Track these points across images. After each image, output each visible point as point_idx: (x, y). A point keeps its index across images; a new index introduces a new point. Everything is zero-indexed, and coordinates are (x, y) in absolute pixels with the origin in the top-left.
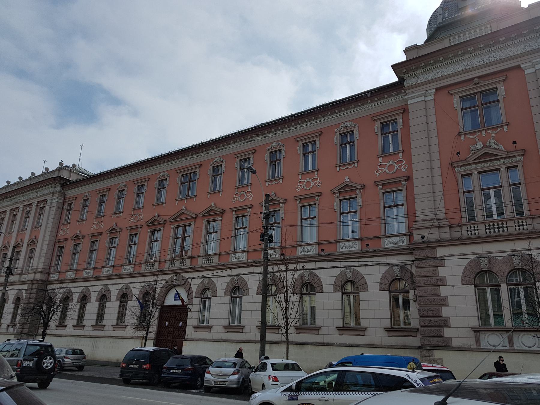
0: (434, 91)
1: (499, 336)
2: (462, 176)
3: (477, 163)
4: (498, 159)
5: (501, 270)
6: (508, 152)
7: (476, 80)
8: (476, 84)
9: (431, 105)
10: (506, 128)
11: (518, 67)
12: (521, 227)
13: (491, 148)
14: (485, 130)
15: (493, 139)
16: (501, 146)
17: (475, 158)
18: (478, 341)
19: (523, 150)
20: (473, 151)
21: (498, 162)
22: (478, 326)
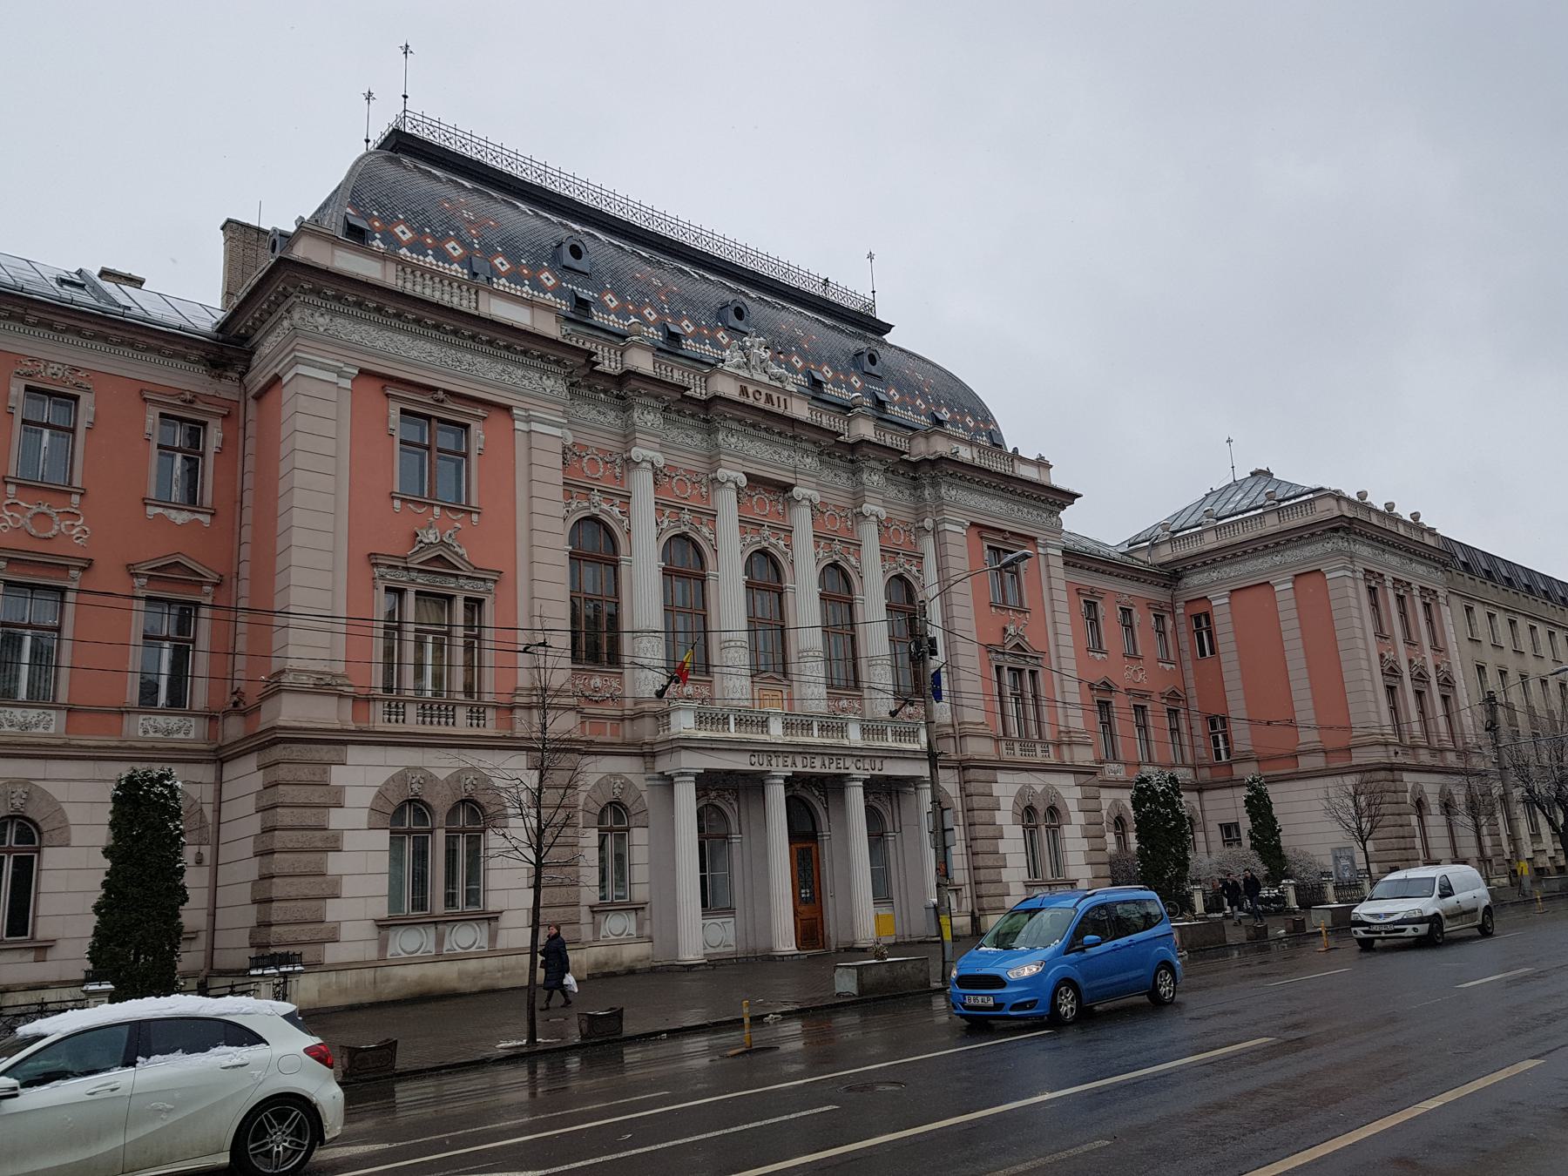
0: (356, 372)
3: (420, 571)
4: (456, 576)
5: (441, 803)
7: (441, 395)
8: (437, 401)
14: (442, 507)
17: (425, 558)
20: (422, 545)
21: (453, 580)
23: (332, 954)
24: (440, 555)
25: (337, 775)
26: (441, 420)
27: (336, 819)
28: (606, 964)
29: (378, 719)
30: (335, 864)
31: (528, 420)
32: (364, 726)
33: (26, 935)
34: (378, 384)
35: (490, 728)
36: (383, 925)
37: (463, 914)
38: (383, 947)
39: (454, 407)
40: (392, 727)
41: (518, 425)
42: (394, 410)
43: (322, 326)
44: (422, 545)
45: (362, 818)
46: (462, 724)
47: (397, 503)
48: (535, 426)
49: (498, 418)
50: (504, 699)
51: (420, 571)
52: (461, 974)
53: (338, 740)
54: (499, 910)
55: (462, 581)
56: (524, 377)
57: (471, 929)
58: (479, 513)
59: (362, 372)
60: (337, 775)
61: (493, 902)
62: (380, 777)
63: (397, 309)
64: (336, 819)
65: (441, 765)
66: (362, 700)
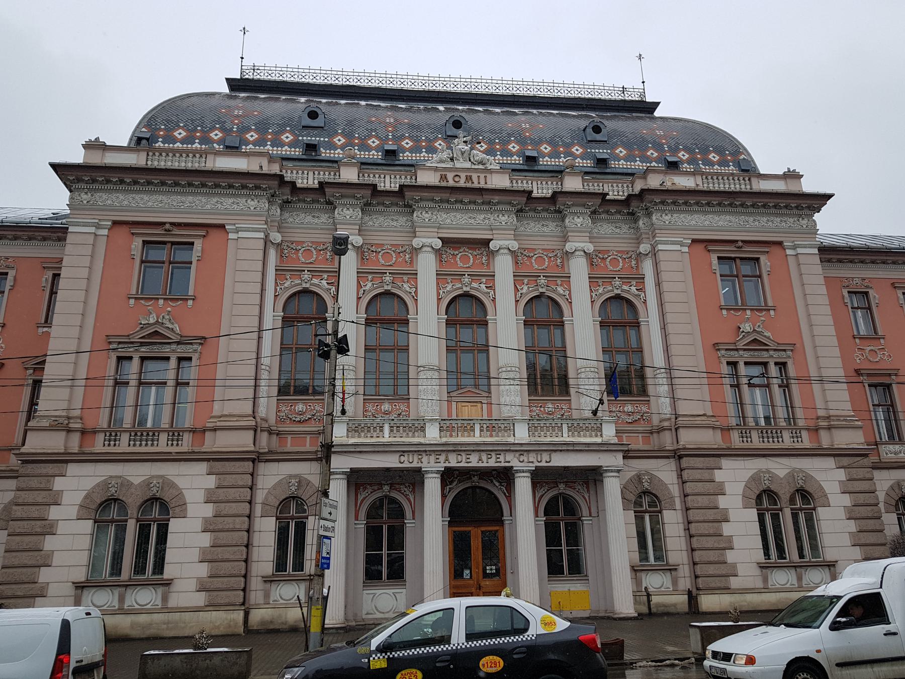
0: (690, 242)
1: (821, 572)
3: (745, 350)
4: (767, 350)
7: (740, 244)
18: (765, 580)
20: (744, 334)
25: (719, 476)
26: (741, 259)
29: (736, 439)
30: (727, 529)
31: (794, 247)
34: (702, 246)
35: (806, 442)
40: (745, 445)
41: (789, 252)
42: (714, 258)
45: (738, 501)
46: (787, 440)
47: (724, 312)
48: (800, 251)
49: (776, 250)
51: (745, 350)
58: (774, 309)
59: (694, 241)
60: (719, 476)
65: (780, 468)
66: (726, 430)
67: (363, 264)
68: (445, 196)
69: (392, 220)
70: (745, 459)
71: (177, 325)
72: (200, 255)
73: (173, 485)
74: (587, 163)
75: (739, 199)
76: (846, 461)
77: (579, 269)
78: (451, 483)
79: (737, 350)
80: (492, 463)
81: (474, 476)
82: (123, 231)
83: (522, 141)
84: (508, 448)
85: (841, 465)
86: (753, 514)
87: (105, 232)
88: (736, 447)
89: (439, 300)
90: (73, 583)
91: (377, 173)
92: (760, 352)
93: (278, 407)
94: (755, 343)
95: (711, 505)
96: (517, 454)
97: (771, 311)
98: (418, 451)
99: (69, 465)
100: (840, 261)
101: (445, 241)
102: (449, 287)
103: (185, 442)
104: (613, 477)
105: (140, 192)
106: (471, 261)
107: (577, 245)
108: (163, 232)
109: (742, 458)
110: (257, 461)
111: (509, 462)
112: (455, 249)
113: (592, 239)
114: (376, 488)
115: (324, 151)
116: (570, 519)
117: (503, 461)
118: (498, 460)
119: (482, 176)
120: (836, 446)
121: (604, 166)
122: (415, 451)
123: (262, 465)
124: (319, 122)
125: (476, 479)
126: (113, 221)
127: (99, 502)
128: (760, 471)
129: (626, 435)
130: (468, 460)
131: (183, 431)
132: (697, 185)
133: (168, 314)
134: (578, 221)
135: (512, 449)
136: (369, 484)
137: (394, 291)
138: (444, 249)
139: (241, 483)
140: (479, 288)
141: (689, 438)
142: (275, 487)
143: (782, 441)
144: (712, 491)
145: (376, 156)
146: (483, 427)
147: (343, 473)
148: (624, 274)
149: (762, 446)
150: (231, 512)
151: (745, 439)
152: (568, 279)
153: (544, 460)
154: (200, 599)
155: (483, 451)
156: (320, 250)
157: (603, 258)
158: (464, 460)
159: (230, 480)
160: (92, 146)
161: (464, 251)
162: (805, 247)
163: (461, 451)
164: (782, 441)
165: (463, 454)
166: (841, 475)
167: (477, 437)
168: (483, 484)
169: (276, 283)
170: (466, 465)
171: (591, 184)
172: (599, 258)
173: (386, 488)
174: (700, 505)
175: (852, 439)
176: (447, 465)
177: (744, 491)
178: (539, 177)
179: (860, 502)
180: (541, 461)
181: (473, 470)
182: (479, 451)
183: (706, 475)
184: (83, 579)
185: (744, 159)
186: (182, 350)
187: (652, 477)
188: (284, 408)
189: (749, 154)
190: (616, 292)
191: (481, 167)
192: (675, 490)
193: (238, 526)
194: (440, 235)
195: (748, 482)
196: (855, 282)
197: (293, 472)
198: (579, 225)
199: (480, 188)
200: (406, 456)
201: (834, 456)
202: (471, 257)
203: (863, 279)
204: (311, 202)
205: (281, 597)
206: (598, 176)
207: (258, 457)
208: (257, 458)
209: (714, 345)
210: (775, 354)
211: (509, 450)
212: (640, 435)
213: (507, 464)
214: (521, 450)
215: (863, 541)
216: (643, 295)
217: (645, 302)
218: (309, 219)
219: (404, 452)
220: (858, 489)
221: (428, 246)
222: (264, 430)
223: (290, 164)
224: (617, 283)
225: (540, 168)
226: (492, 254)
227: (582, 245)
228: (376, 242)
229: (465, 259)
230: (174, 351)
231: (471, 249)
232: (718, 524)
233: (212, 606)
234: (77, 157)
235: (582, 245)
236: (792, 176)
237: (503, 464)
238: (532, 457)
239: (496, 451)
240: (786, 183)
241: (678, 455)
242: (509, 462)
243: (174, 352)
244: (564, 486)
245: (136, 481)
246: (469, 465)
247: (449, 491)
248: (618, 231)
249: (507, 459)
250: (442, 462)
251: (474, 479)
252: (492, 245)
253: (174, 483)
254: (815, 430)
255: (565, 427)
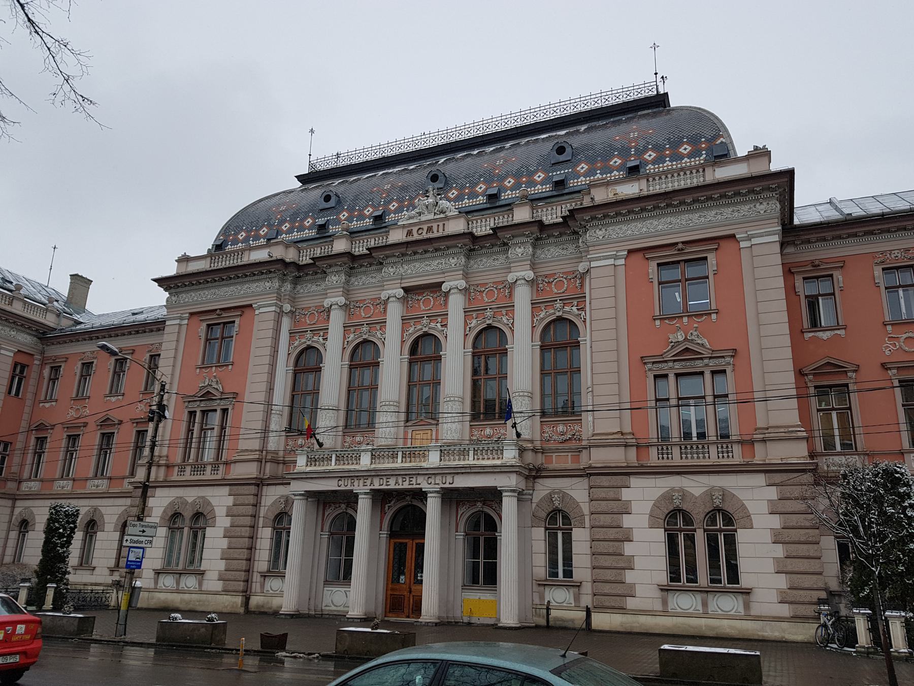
0: (626, 253)
2: (656, 377)
3: (675, 361)
4: (701, 359)
6: (713, 351)
7: (680, 246)
8: (679, 250)
9: (621, 271)
10: (714, 316)
11: (733, 236)
12: (725, 455)
13: (693, 343)
14: (688, 316)
15: (695, 331)
16: (706, 340)
17: (675, 353)
19: (733, 349)
20: (673, 344)
22: (666, 584)
23: (631, 603)
24: (687, 348)
25: (626, 494)
26: (686, 261)
27: (627, 521)
28: (263, 606)
29: (653, 457)
30: (628, 549)
31: (749, 238)
32: (643, 462)
33: (728, 584)
34: (640, 255)
35: (737, 456)
36: (664, 590)
37: (724, 587)
38: (665, 602)
39: (693, 252)
41: (743, 244)
42: (653, 265)
43: (761, 210)
44: (673, 344)
45: (645, 520)
46: (713, 456)
47: (658, 322)
48: (754, 241)
49: (726, 245)
50: (748, 438)
51: (675, 361)
52: (182, 600)
53: (627, 472)
54: (750, 587)
55: (706, 361)
56: (700, 217)
57: (729, 598)
58: (717, 313)
59: (630, 252)
60: (626, 494)
61: (95, 563)
62: (658, 493)
63: (603, 213)
64: (627, 521)
65: (696, 486)
66: (639, 447)
67: (350, 319)
68: (403, 250)
69: (372, 277)
70: (656, 476)
71: (220, 386)
72: (237, 330)
73: (209, 503)
74: (546, 188)
75: (675, 199)
76: (778, 478)
77: (522, 297)
78: (390, 502)
79: (666, 362)
80: (406, 485)
81: (407, 495)
82: (195, 319)
83: (489, 182)
84: (417, 472)
85: (772, 482)
86: (660, 535)
87: (186, 322)
88: (652, 465)
89: (403, 342)
90: (108, 568)
91: (361, 239)
92: (692, 362)
93: (542, 429)
94: (688, 351)
95: (614, 524)
96: (426, 477)
97: (712, 315)
98: (352, 476)
99: (157, 489)
100: (871, 233)
101: (406, 290)
102: (412, 330)
103: (220, 472)
104: (507, 496)
105: (203, 289)
106: (432, 303)
107: (518, 274)
108: (216, 317)
109: (654, 477)
110: (261, 485)
111: (420, 484)
112: (419, 294)
113: (533, 267)
114: (337, 506)
115: (331, 228)
116: (489, 534)
117: (415, 484)
118: (411, 483)
119: (441, 224)
120: (767, 462)
121: (562, 187)
122: (350, 477)
123: (265, 488)
124: (332, 203)
125: (408, 498)
126: (190, 313)
127: (170, 515)
128: (673, 489)
129: (556, 454)
130: (388, 483)
131: (207, 464)
132: (641, 190)
133: (215, 378)
134: (520, 251)
135: (420, 472)
136: (333, 503)
137: (371, 339)
138: (410, 296)
139: (247, 502)
140: (435, 327)
141: (600, 457)
142: (271, 505)
143: (709, 457)
144: (615, 510)
145: (368, 222)
146: (405, 454)
147: (300, 495)
148: (565, 296)
149: (685, 462)
150: (241, 523)
151: (701, 455)
152: (512, 308)
153: (448, 483)
154: (218, 586)
155: (399, 475)
156: (321, 312)
157: (549, 282)
158: (385, 484)
159: (241, 499)
160: (184, 259)
161: (427, 295)
162: (761, 235)
163: (383, 475)
164: (709, 457)
165: (384, 478)
166: (773, 493)
167: (399, 464)
168: (415, 503)
169: (290, 343)
170: (386, 487)
171: (545, 209)
172: (546, 282)
173: (343, 506)
174: (601, 523)
175: (797, 452)
176: (372, 487)
177: (651, 510)
178: (494, 213)
179: (791, 524)
180: (445, 483)
181: (406, 491)
182: (396, 475)
183: (611, 494)
184: (159, 568)
185: (722, 142)
186: (223, 404)
187: (564, 496)
188: (547, 430)
189: (729, 136)
190: (558, 314)
191: (442, 216)
192: (586, 511)
193: (243, 534)
194: (403, 285)
195: (657, 501)
196: (893, 256)
197: (200, 495)
198: (520, 255)
199: (427, 239)
200: (343, 480)
201: (766, 472)
202: (432, 300)
203: (907, 250)
204: (368, 266)
205: (271, 589)
206: (553, 200)
207: (261, 482)
208: (260, 483)
209: (642, 357)
210: (712, 362)
211: (419, 474)
212: (570, 454)
213: (418, 486)
214: (430, 473)
215: (789, 568)
216: (584, 314)
217: (585, 321)
218: (314, 288)
219: (341, 477)
220: (790, 510)
221: (393, 297)
222: (268, 461)
223: (304, 245)
224: (558, 305)
225: (501, 203)
226: (447, 294)
227: (523, 273)
228: (359, 299)
229: (426, 302)
230: (219, 405)
231: (432, 292)
232: (619, 543)
233: (226, 591)
234: (171, 270)
235: (523, 273)
236: (761, 153)
237: (415, 486)
238: (438, 480)
239: (409, 474)
240: (749, 165)
241: (587, 473)
242: (420, 484)
243: (218, 405)
244: (481, 504)
245: (190, 500)
246: (389, 487)
247: (388, 509)
248: (565, 252)
249: (418, 482)
250: (369, 485)
251: (407, 498)
252: (444, 288)
253: (209, 502)
254: (748, 443)
255: (471, 453)
